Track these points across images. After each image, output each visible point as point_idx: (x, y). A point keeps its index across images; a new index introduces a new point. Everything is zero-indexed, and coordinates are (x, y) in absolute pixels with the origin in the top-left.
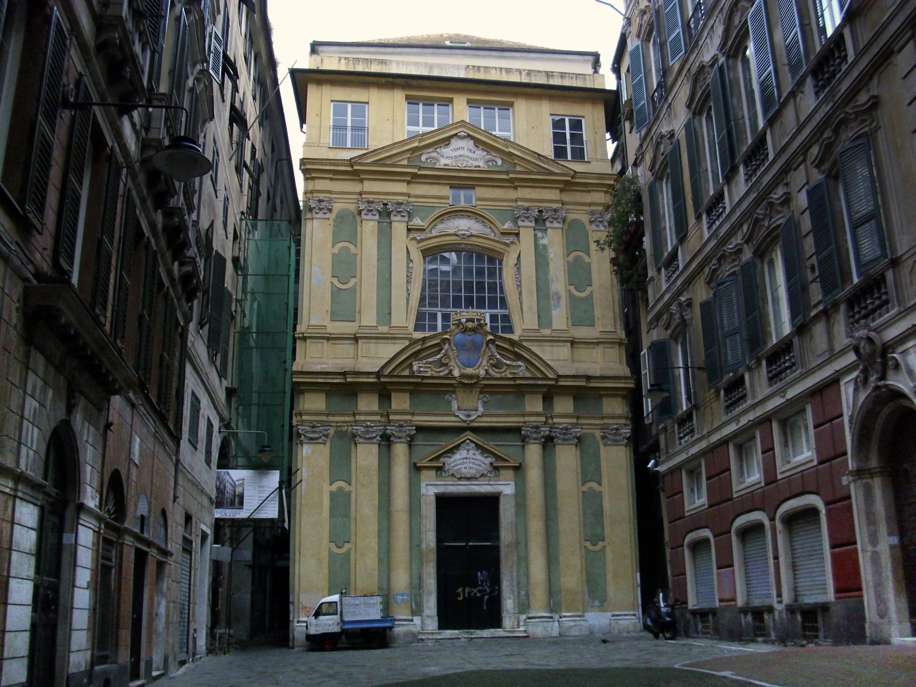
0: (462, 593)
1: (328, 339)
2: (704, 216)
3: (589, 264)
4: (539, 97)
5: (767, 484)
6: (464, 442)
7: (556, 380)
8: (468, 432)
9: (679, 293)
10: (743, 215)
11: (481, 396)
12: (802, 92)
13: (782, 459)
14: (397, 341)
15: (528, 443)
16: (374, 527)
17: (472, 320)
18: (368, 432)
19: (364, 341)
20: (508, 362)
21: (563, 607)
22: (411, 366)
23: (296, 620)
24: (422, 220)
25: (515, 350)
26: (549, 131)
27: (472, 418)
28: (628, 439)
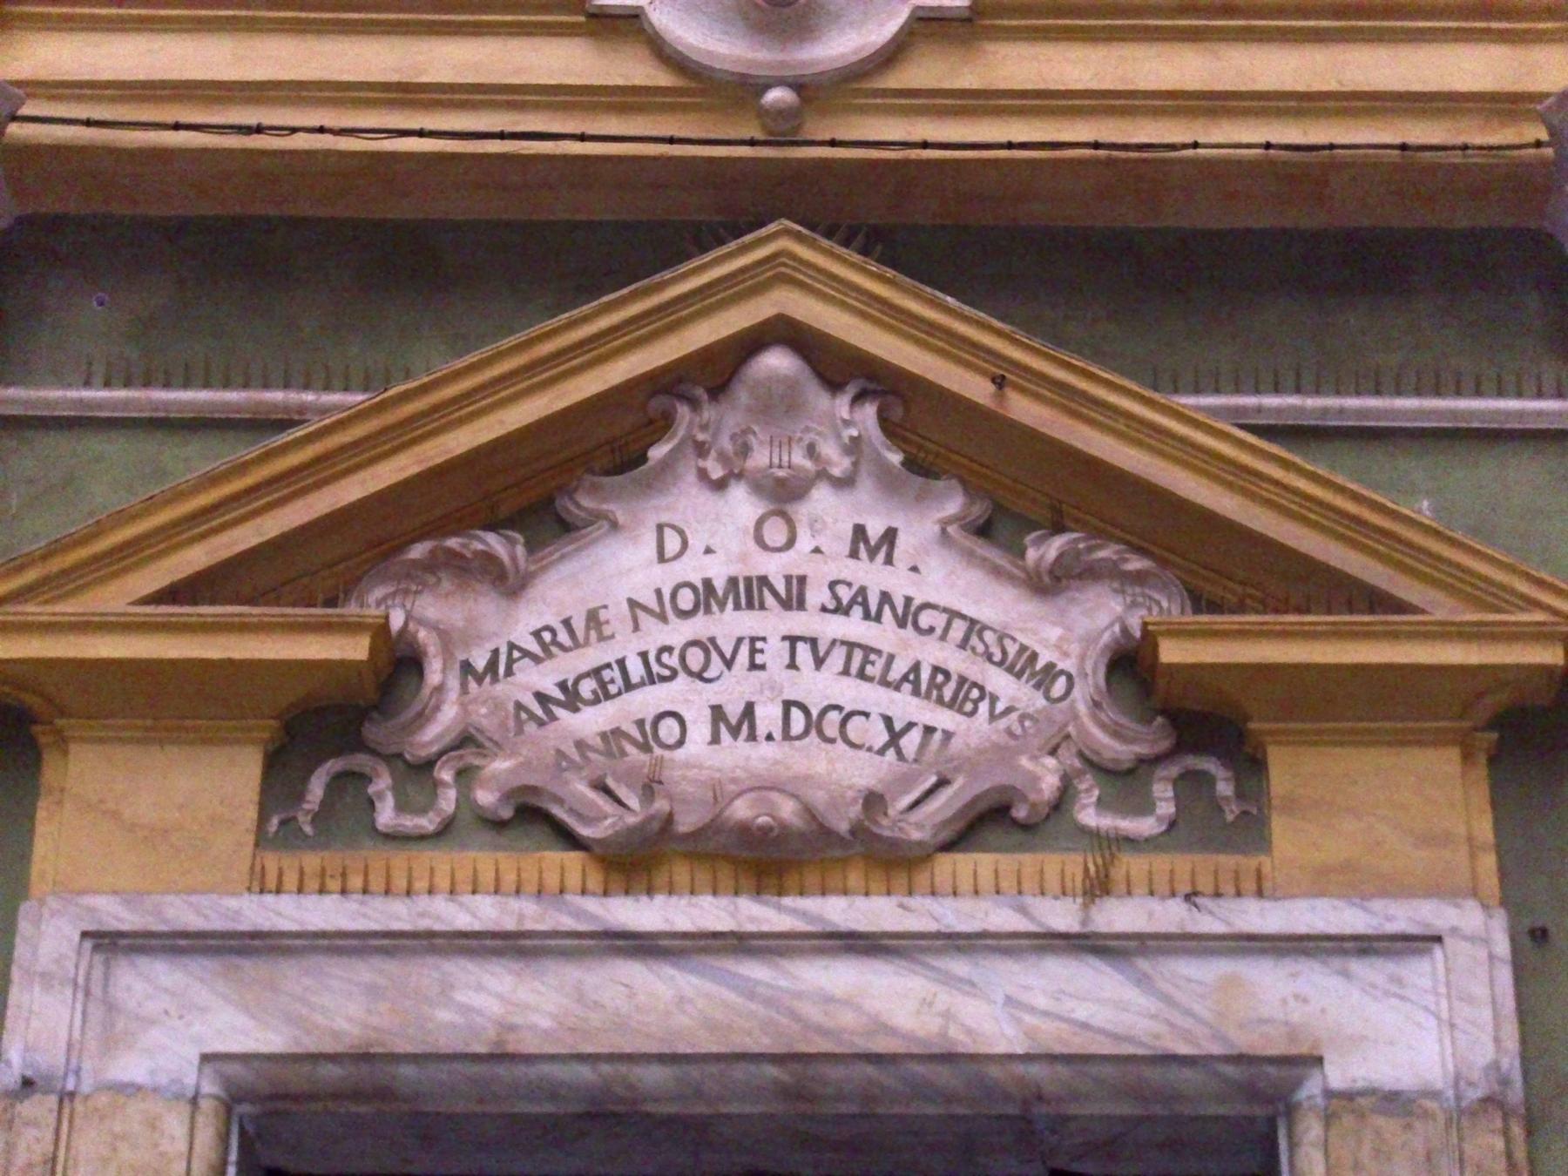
6: (718, 370)
8: (780, 240)
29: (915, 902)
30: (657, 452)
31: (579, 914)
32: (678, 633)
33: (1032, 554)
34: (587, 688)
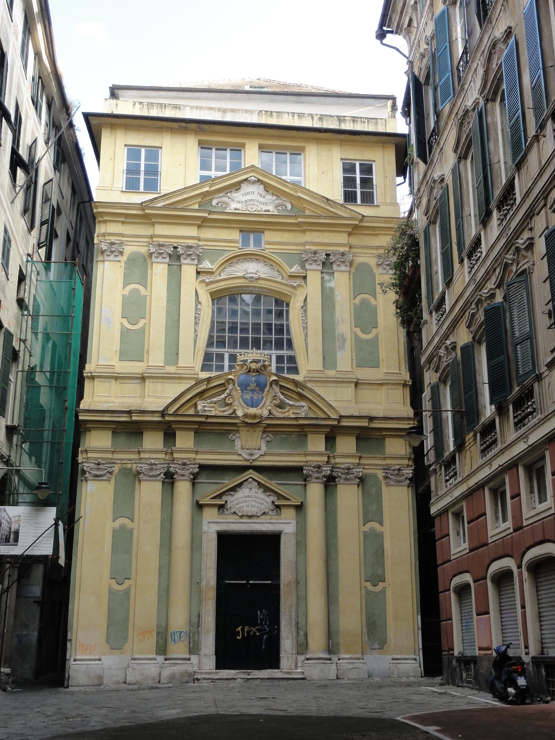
0: (241, 632)
1: (116, 378)
2: (466, 260)
3: (375, 308)
4: (329, 142)
5: (515, 530)
6: (246, 480)
7: (339, 421)
8: (251, 471)
9: (446, 336)
10: (496, 259)
11: (264, 436)
12: (544, 136)
13: (528, 504)
14: (183, 381)
16: (154, 564)
17: (256, 361)
18: (152, 469)
19: (151, 380)
20: (291, 403)
21: (342, 648)
22: (195, 405)
23: (72, 659)
24: (212, 263)
25: (299, 391)
26: (339, 175)
27: (255, 457)
28: (410, 479)
32: (244, 499)
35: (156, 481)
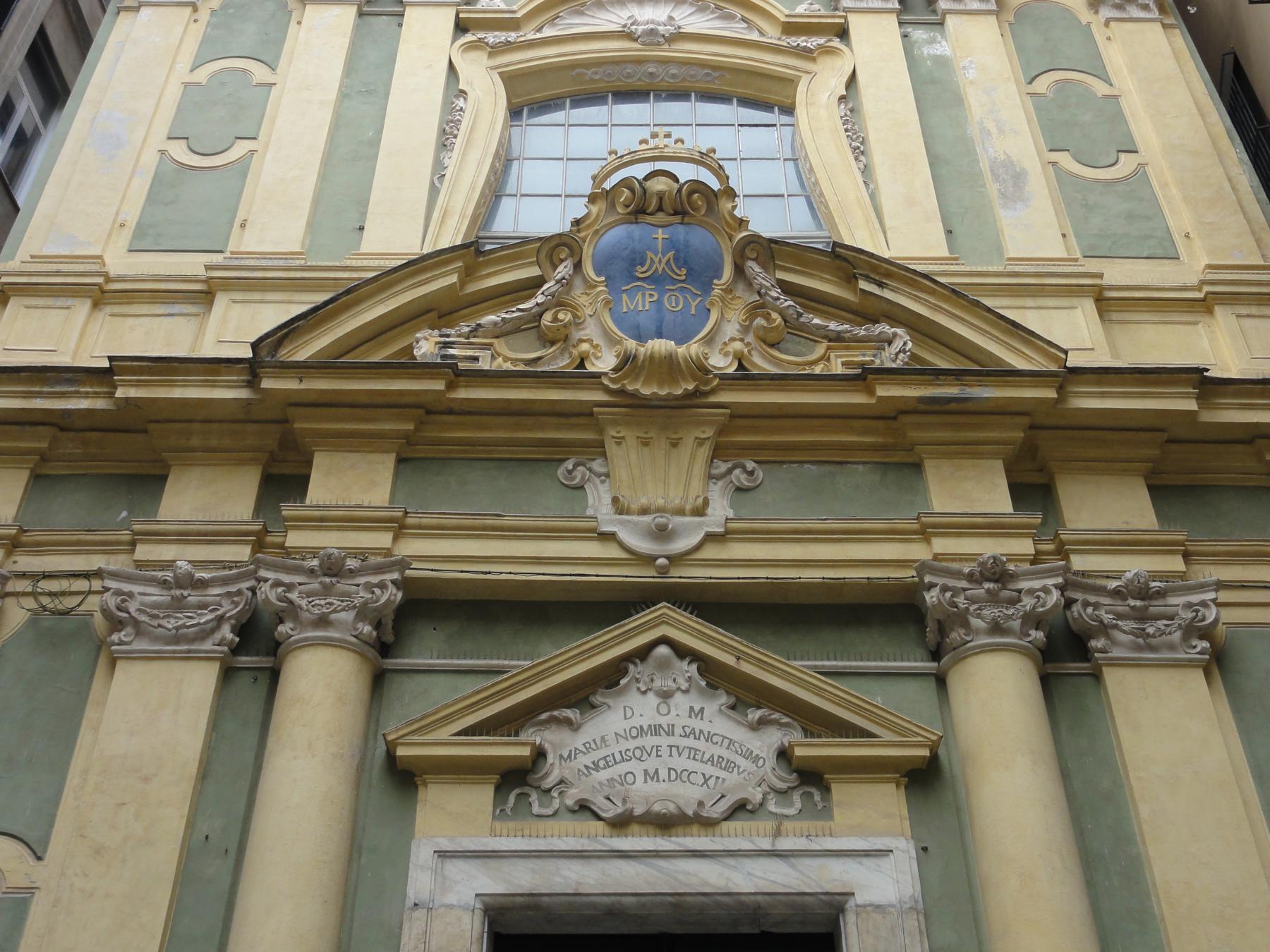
6: (643, 654)
8: (663, 609)
11: (722, 467)
15: (963, 653)
18: (178, 605)
27: (681, 545)
29: (715, 839)
30: (623, 682)
31: (602, 844)
32: (632, 744)
33: (750, 717)
34: (602, 763)
35: (188, 657)
